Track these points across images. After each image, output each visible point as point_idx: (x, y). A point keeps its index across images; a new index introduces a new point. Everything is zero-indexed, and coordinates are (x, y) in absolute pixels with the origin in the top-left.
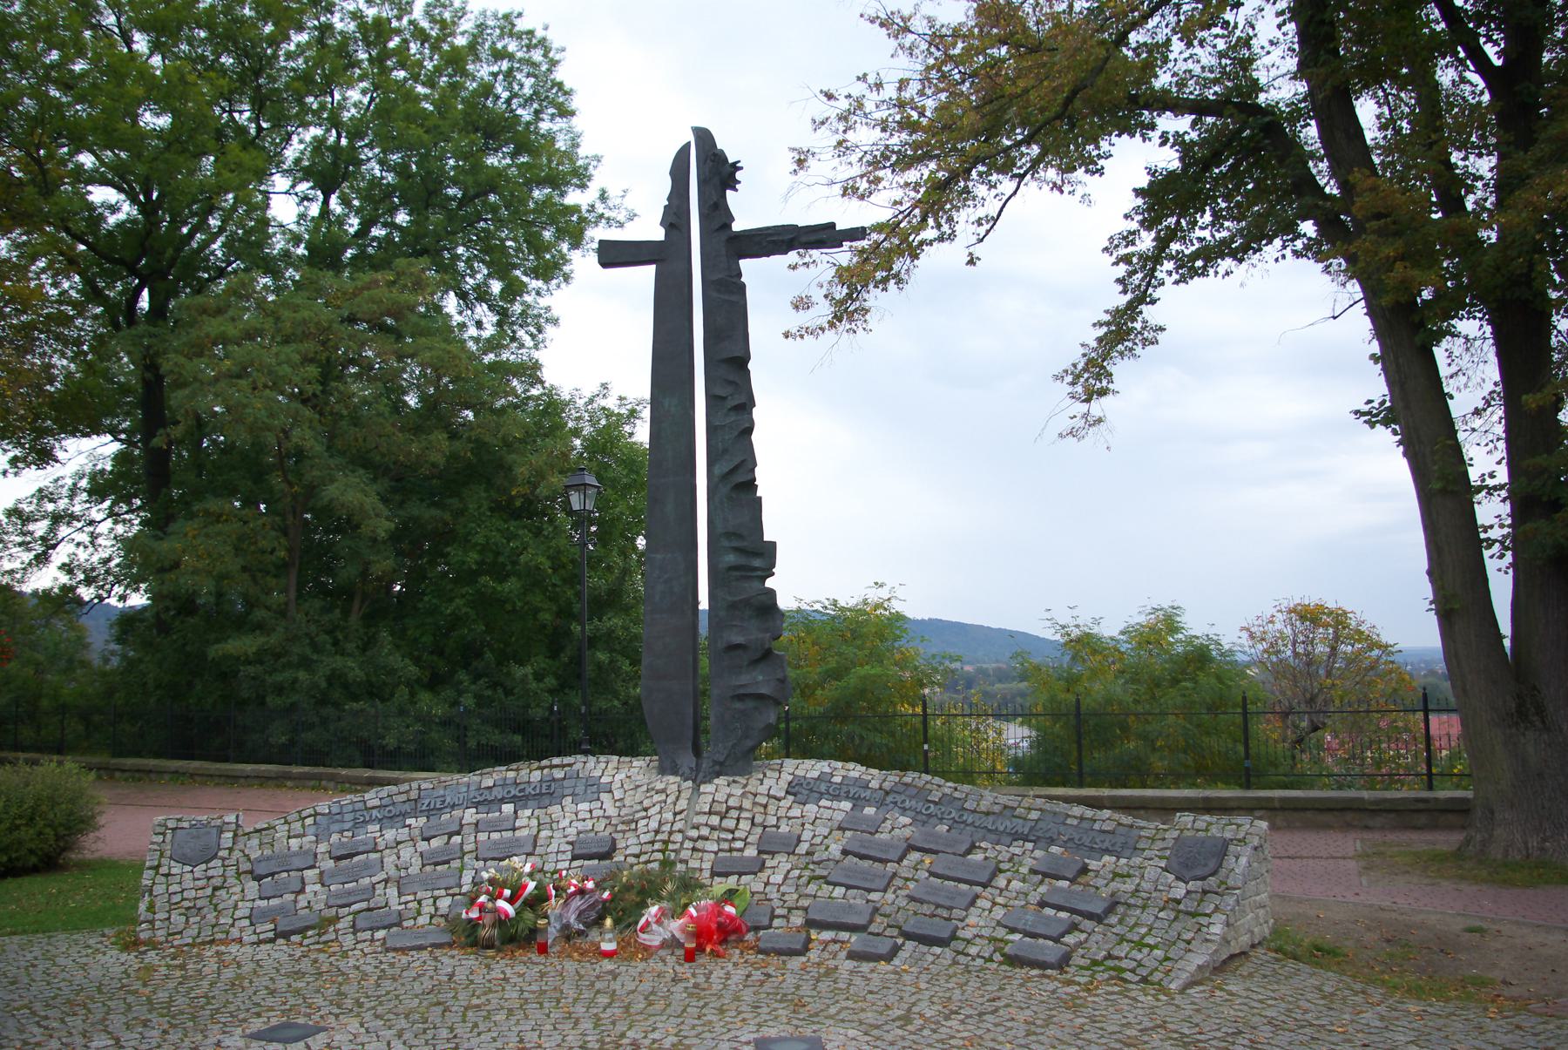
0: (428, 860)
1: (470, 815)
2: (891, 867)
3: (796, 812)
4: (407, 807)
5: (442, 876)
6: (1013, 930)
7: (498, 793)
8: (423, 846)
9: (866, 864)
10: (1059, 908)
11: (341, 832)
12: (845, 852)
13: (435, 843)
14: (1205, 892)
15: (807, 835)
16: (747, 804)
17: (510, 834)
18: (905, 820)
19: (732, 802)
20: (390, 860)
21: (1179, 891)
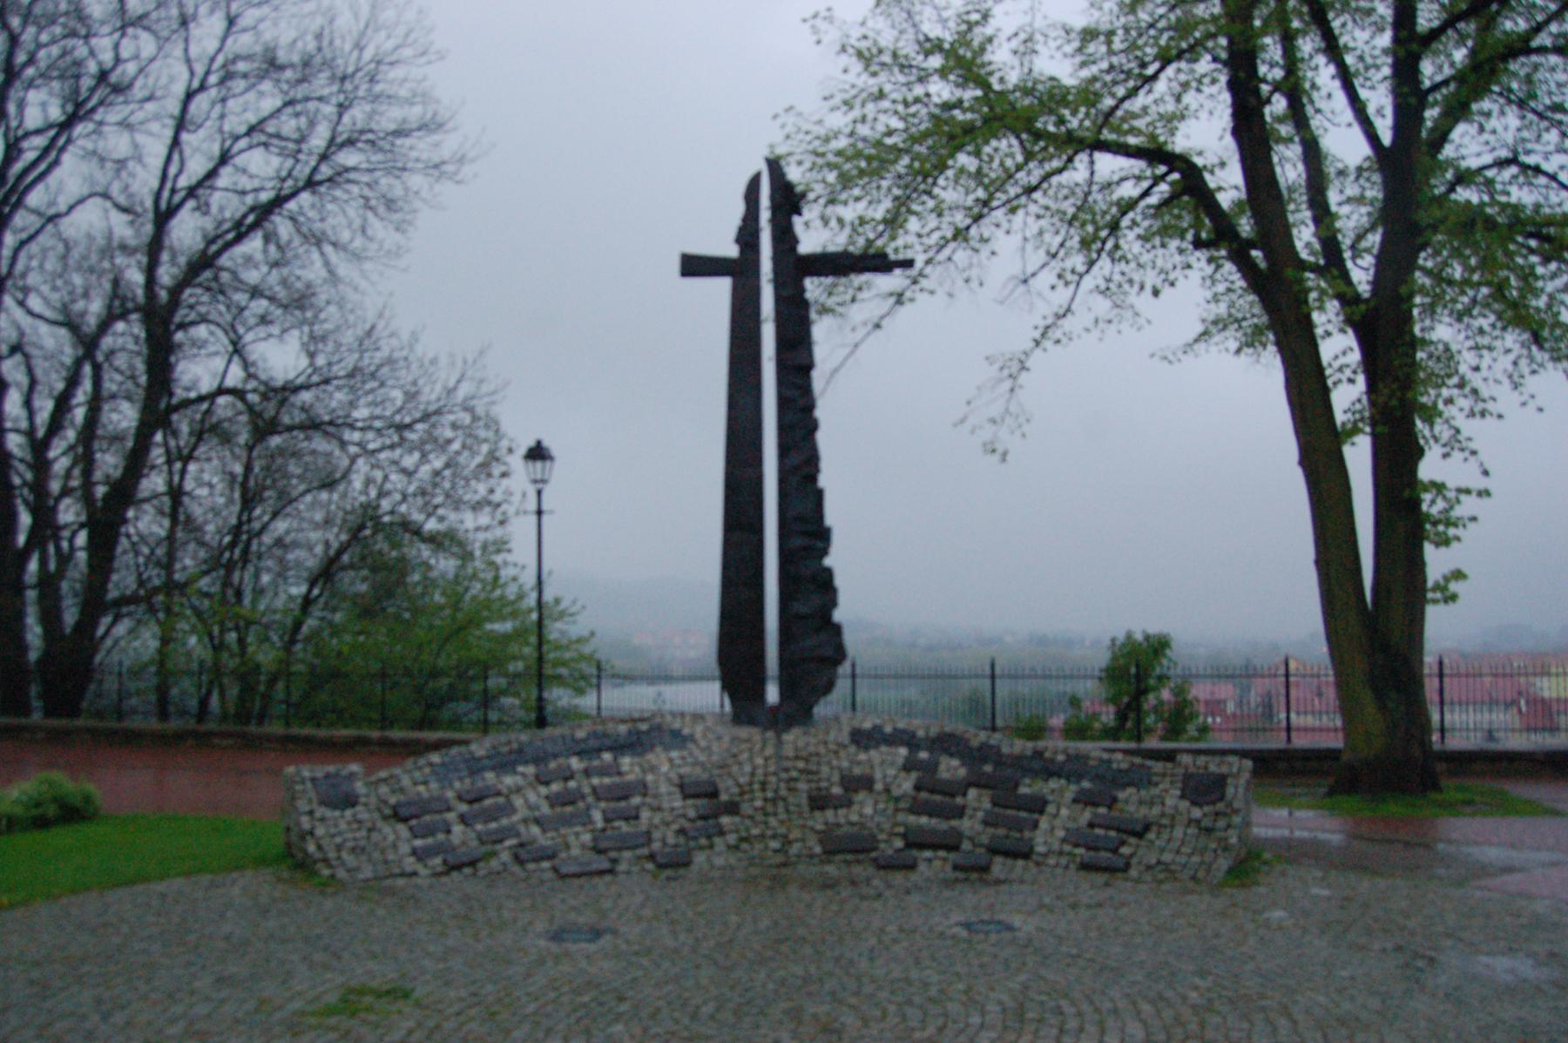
0: (553, 801)
1: (575, 763)
2: (959, 800)
3: (862, 756)
4: (513, 757)
5: (572, 816)
6: (1077, 845)
7: (593, 743)
8: (543, 790)
9: (938, 798)
10: (1108, 828)
11: (461, 779)
12: (917, 788)
13: (555, 787)
14: (1217, 814)
15: (878, 775)
16: (822, 750)
17: (616, 779)
18: (955, 762)
19: (812, 749)
20: (518, 802)
21: (1197, 813)
